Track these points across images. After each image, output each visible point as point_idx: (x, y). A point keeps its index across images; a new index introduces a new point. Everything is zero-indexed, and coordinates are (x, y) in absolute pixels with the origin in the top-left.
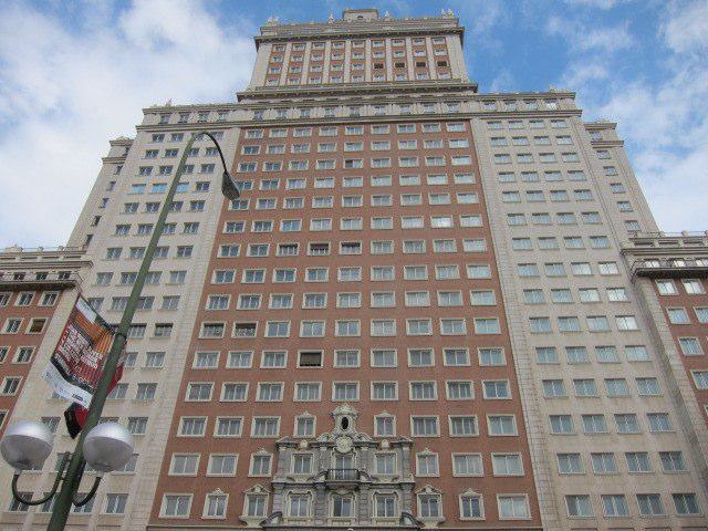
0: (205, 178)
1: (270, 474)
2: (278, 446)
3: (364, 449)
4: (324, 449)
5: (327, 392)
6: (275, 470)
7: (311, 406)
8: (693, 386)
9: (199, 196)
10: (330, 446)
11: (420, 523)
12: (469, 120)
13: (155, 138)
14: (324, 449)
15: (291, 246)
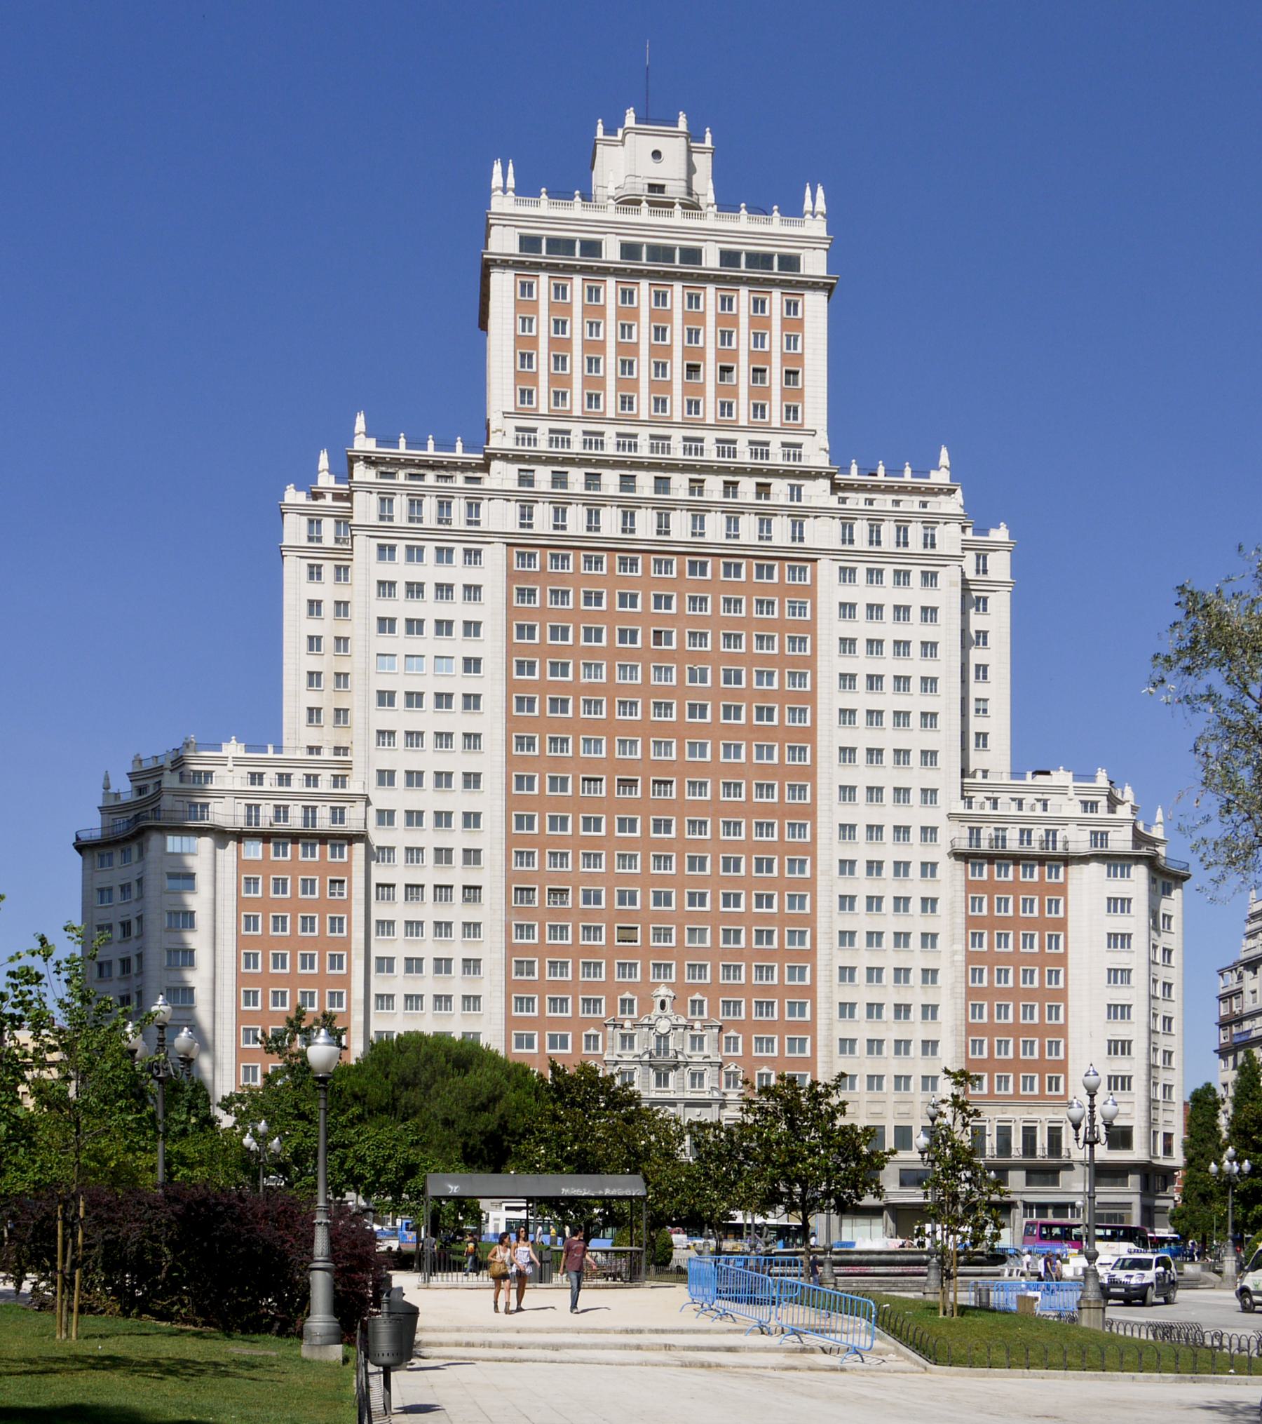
0: (471, 648)
1: (600, 1051)
2: (606, 1025)
3: (681, 1030)
4: (646, 1030)
5: (645, 972)
6: (604, 1049)
7: (632, 987)
8: (967, 982)
9: (471, 684)
10: (651, 1027)
11: (724, 1094)
12: (815, 560)
13: (381, 548)
14: (646, 1030)
15: (596, 780)
